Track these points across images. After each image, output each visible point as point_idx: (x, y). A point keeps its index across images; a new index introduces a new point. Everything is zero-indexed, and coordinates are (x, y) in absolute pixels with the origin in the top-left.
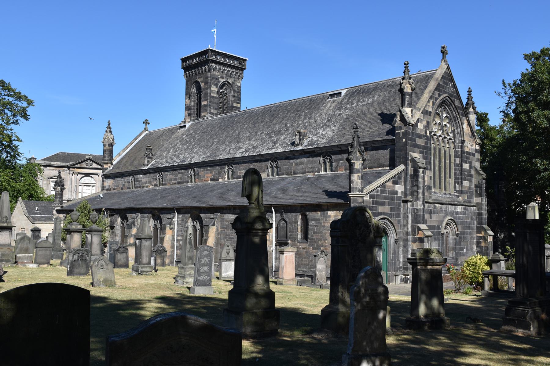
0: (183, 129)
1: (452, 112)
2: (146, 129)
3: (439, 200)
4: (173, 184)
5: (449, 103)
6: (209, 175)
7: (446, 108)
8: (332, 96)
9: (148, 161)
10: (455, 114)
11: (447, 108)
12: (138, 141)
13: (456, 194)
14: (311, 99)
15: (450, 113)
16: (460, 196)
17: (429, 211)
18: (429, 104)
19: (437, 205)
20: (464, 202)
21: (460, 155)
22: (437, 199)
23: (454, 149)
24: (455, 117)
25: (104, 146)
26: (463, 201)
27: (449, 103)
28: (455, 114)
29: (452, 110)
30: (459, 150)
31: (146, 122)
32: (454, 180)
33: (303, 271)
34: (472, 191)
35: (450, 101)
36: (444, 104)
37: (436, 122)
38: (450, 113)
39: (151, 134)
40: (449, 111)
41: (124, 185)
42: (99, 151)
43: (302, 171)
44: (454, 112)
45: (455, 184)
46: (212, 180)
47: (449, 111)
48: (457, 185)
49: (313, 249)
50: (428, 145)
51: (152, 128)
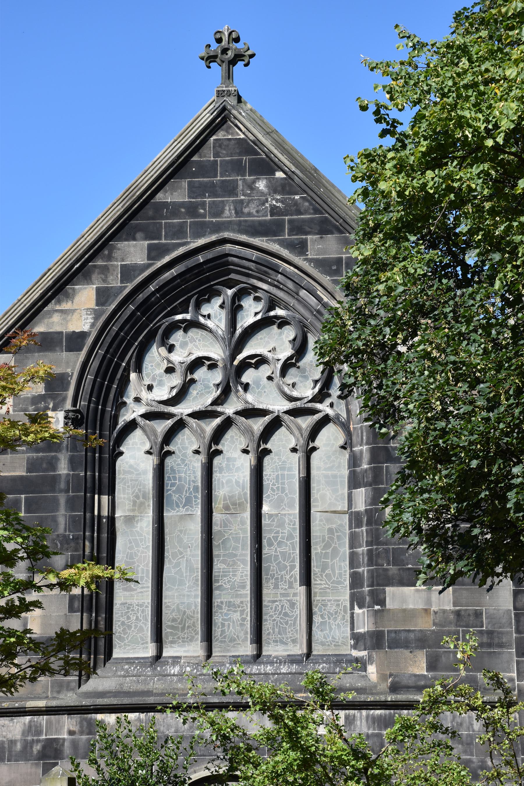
1: (295, 295)
3: (149, 693)
5: (252, 265)
7: (256, 289)
10: (312, 301)
11: (265, 286)
13: (356, 653)
15: (292, 302)
16: (370, 660)
17: (37, 748)
18: (66, 306)
19: (110, 719)
20: (394, 688)
21: (366, 470)
22: (140, 687)
23: (343, 447)
24: (318, 312)
26: (384, 686)
27: (252, 265)
28: (312, 301)
29: (290, 285)
30: (365, 448)
32: (352, 587)
34: (490, 633)
35: (254, 255)
36: (233, 276)
37: (169, 361)
38: (292, 302)
40: (280, 294)
44: (303, 293)
45: (352, 608)
47: (280, 294)
48: (357, 610)
50: (52, 464)
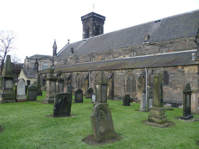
0: (85, 41)
2: (69, 43)
4: (83, 62)
6: (100, 57)
8: (156, 22)
9: (72, 54)
12: (66, 47)
14: (145, 24)
25: (53, 49)
31: (69, 40)
33: (166, 100)
39: (71, 44)
41: (61, 64)
42: (50, 53)
43: (148, 53)
46: (101, 59)
49: (172, 89)
51: (70, 43)
